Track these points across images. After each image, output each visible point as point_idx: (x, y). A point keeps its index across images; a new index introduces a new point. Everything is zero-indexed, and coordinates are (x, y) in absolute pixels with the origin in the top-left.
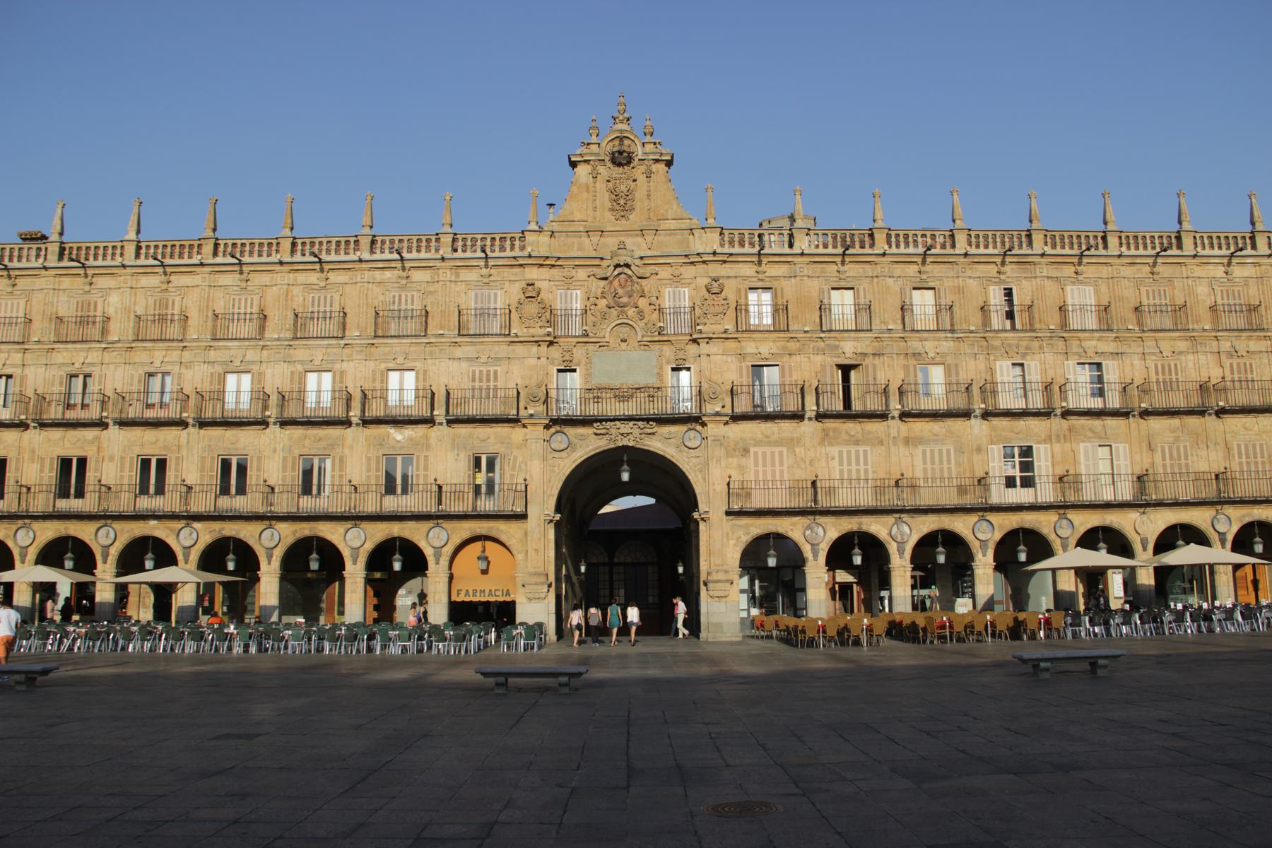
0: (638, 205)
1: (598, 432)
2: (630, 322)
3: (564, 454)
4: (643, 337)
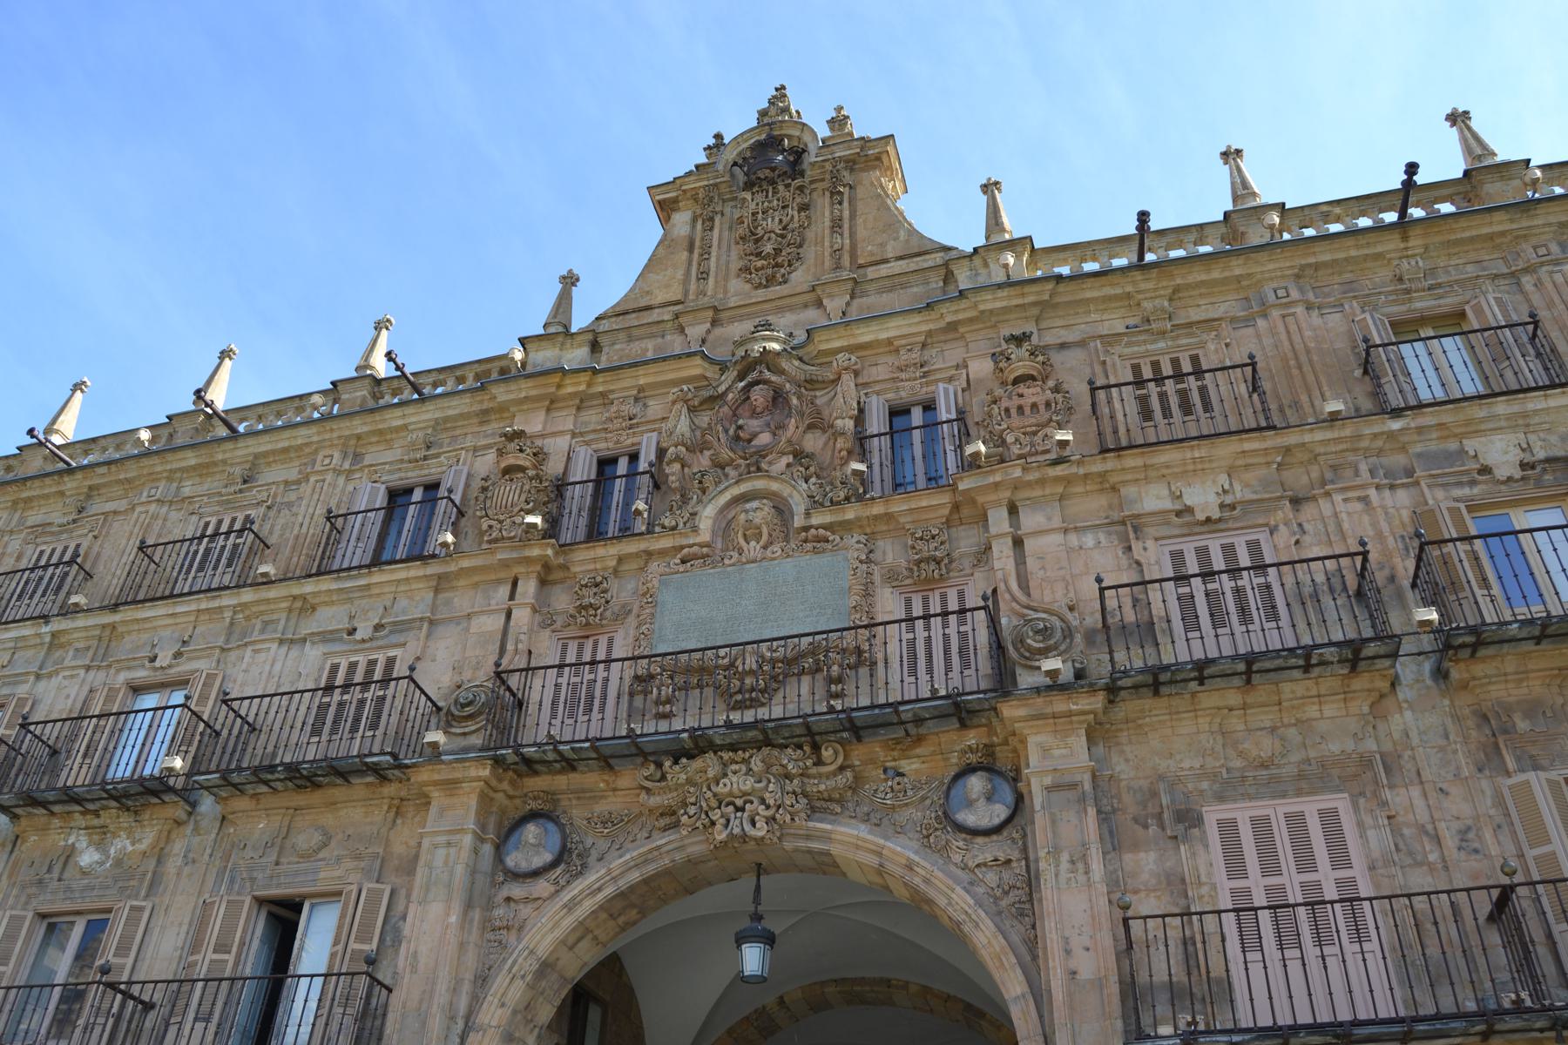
0: (809, 252)
1: (654, 801)
2: (775, 486)
3: (542, 887)
4: (808, 514)
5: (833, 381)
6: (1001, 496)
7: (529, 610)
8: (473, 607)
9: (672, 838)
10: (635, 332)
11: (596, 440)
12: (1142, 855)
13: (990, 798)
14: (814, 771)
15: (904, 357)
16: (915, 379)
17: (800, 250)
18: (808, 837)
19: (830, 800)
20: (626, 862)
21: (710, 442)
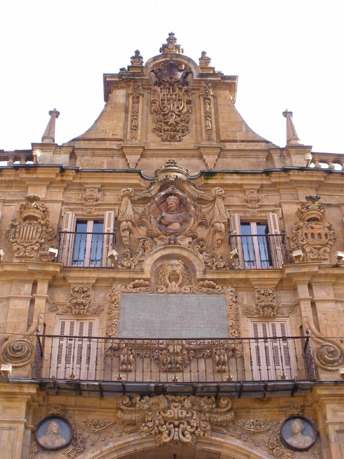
0: (192, 127)
1: (127, 417)
2: (185, 254)
4: (205, 272)
5: (211, 201)
6: (306, 279)
7: (45, 301)
8: (10, 293)
9: (136, 438)
10: (97, 152)
11: (77, 209)
13: (302, 432)
14: (215, 410)
15: (249, 195)
16: (255, 208)
17: (187, 125)
18: (210, 444)
19: (221, 426)
20: (110, 449)
21: (145, 223)
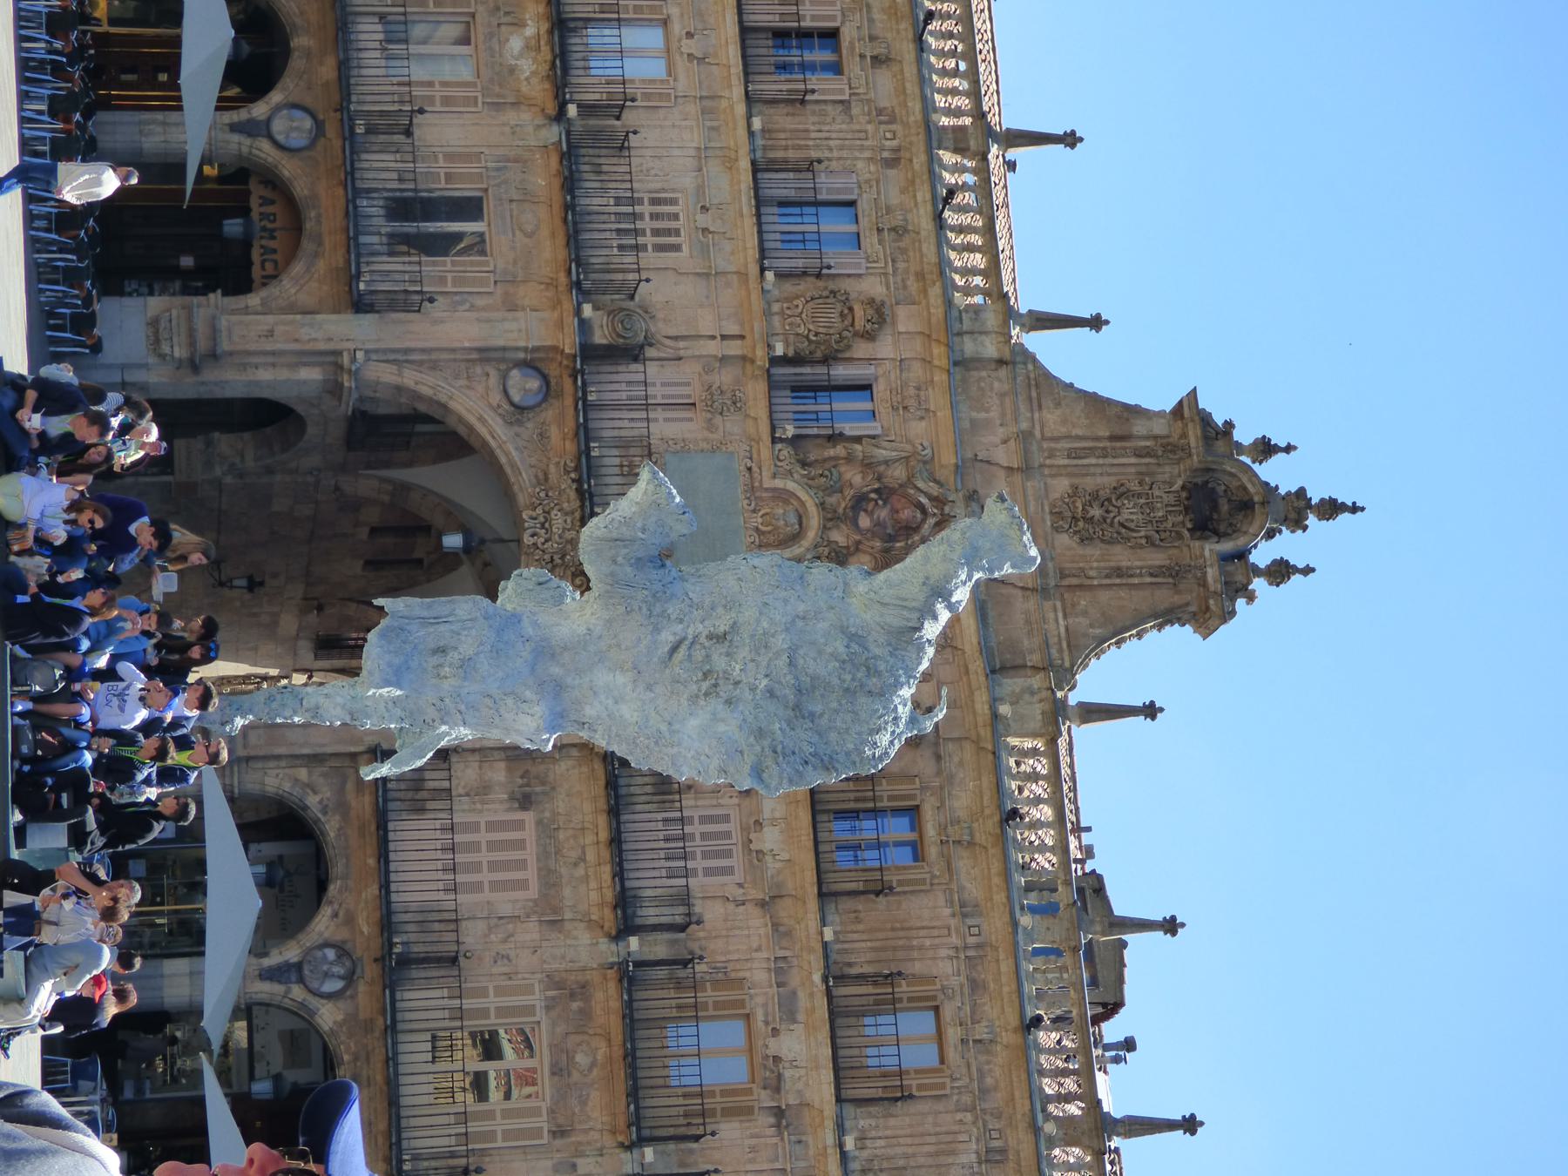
1: (552, 469)
2: (811, 535)
3: (496, 398)
12: (503, 773)
